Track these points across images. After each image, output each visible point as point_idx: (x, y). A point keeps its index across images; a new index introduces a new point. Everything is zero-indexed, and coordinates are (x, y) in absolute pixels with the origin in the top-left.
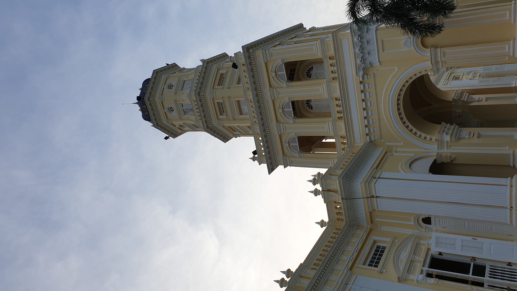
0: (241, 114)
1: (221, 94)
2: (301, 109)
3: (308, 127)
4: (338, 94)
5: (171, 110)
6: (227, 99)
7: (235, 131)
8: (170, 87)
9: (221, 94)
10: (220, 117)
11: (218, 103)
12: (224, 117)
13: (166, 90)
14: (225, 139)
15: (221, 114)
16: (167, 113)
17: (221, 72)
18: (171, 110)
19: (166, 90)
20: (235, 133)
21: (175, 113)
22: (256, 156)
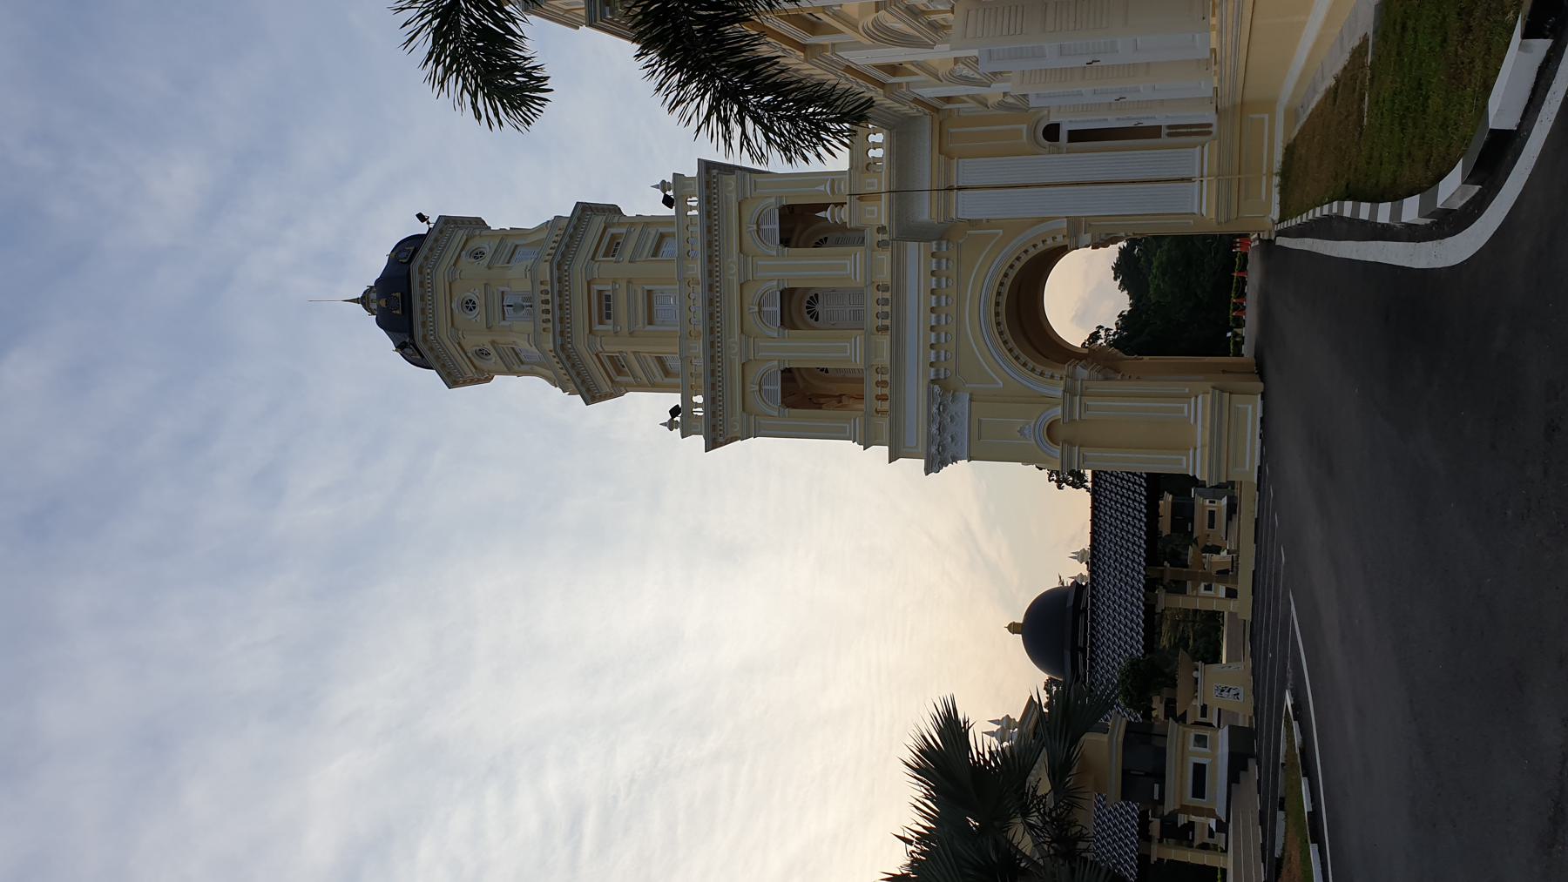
0: (650, 323)
1: (609, 273)
2: (798, 307)
3: (807, 349)
4: (885, 276)
5: (470, 305)
6: (624, 285)
7: (619, 372)
8: (478, 255)
9: (609, 273)
10: (597, 327)
11: (600, 292)
12: (608, 326)
13: (465, 261)
14: (591, 397)
15: (601, 323)
16: (456, 311)
17: (612, 231)
18: (470, 305)
19: (465, 261)
20: (618, 379)
21: (478, 316)
22: (677, 419)
